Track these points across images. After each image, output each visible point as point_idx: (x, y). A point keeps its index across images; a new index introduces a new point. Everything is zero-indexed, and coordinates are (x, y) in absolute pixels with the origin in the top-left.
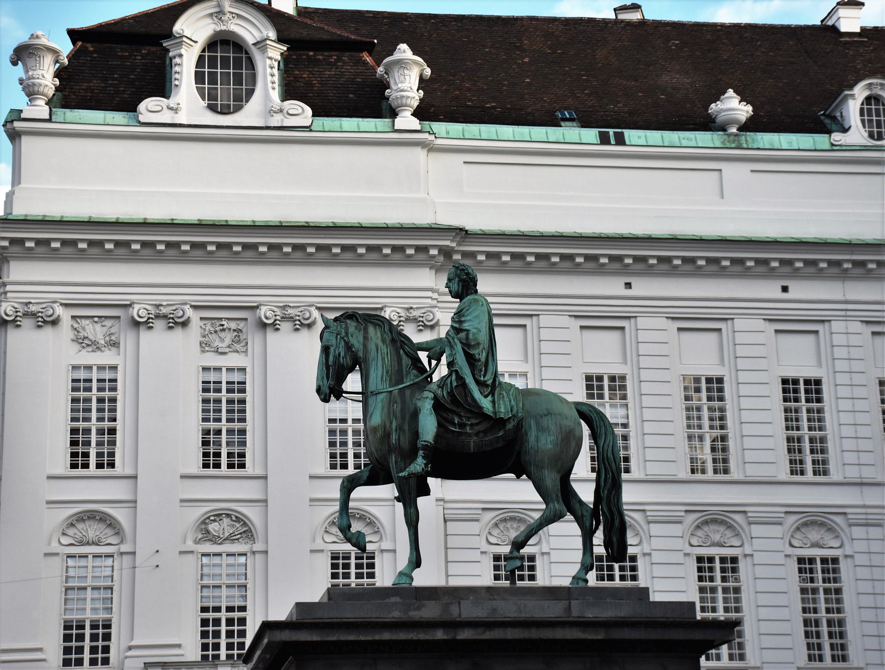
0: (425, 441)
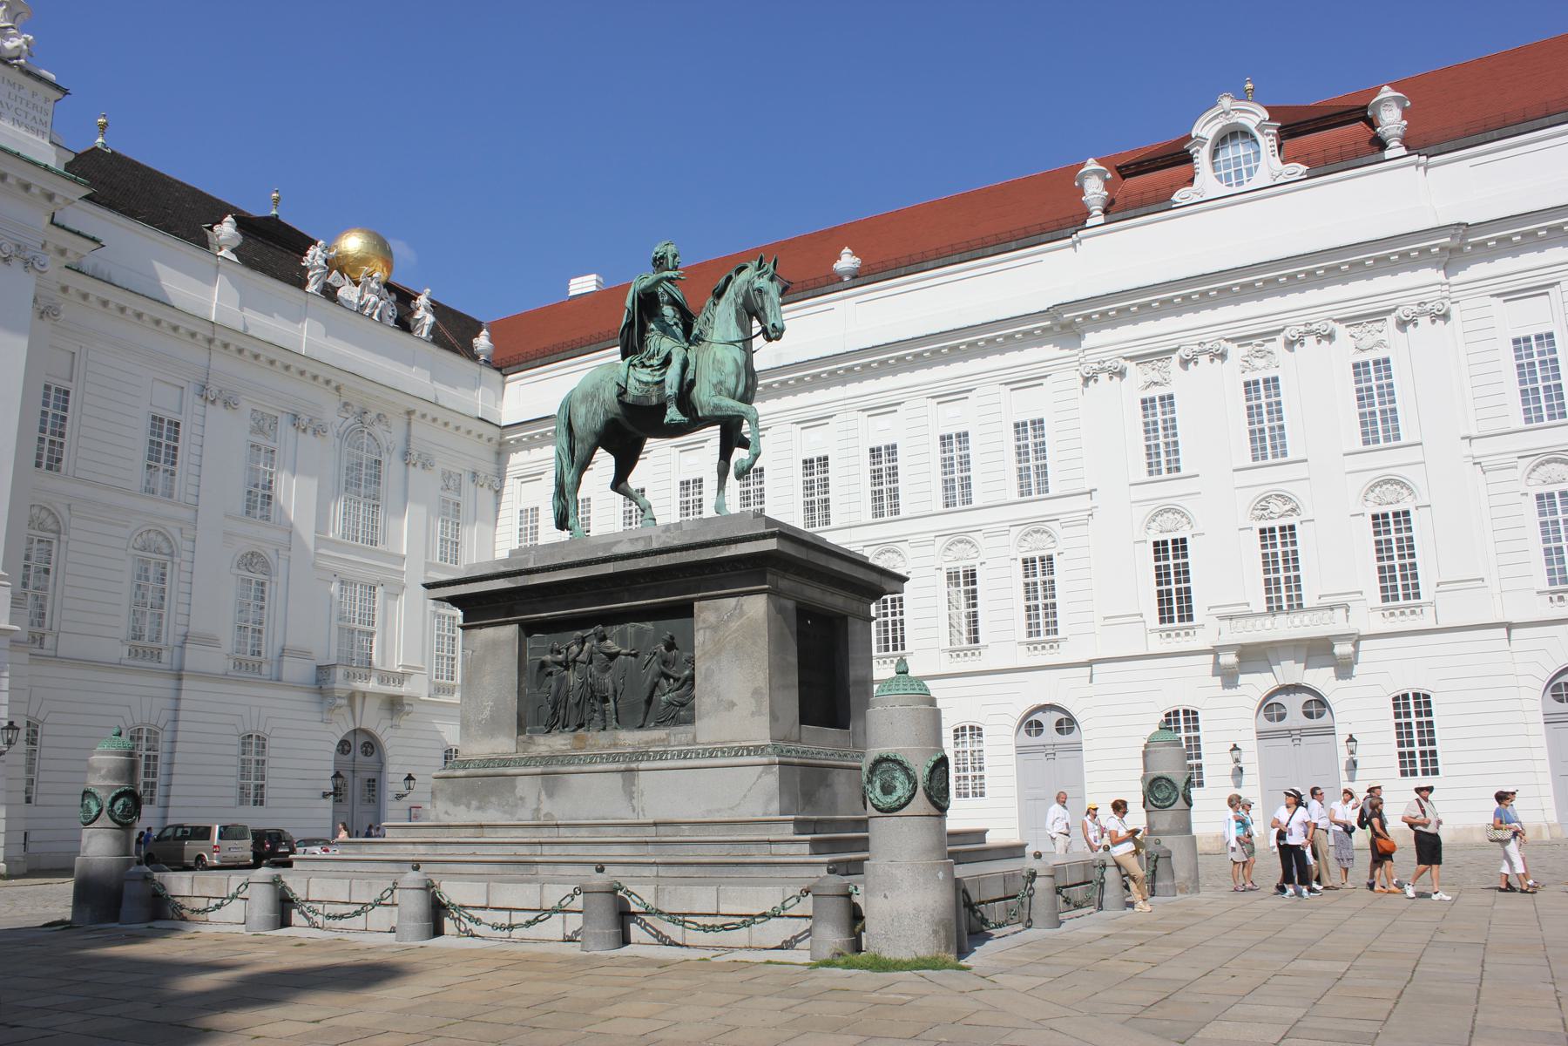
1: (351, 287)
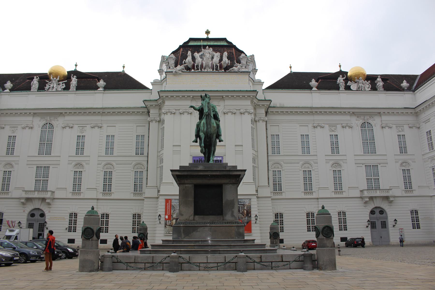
1: (355, 84)
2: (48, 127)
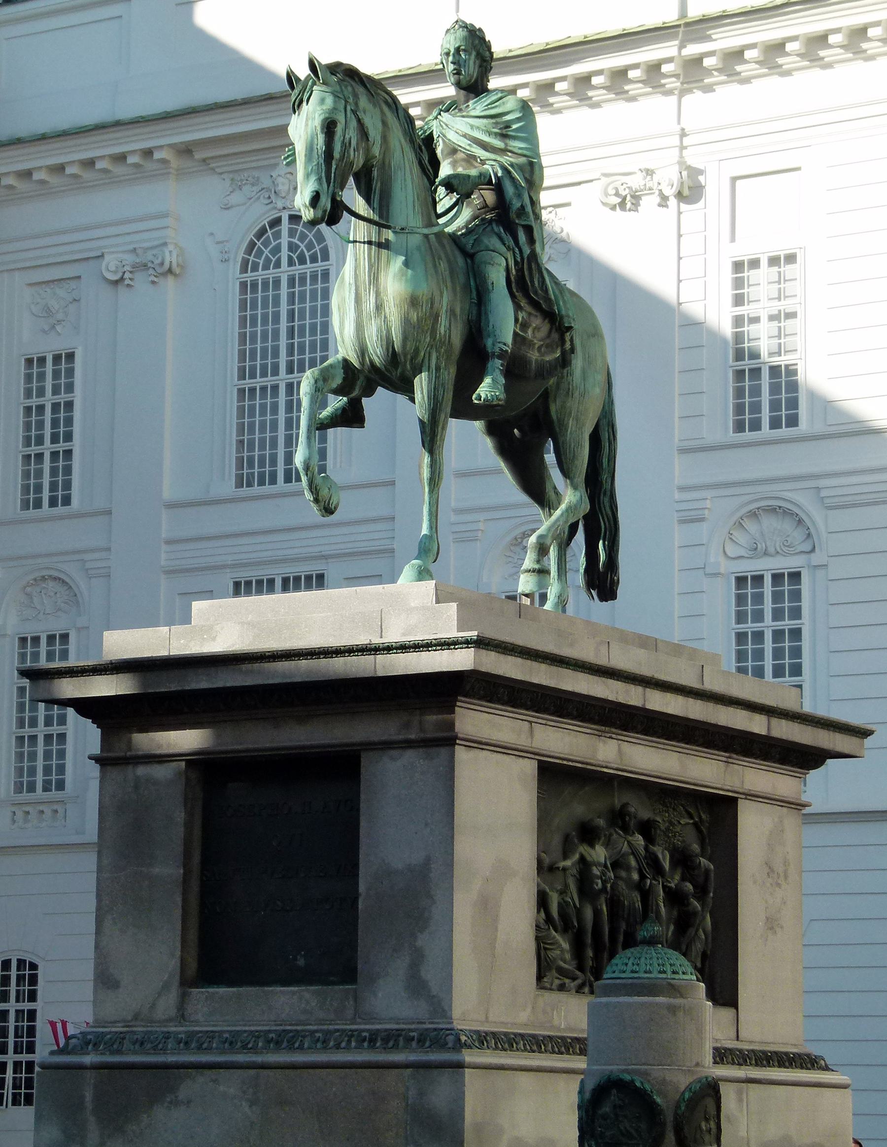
0: (505, 344)
2: (284, 253)
